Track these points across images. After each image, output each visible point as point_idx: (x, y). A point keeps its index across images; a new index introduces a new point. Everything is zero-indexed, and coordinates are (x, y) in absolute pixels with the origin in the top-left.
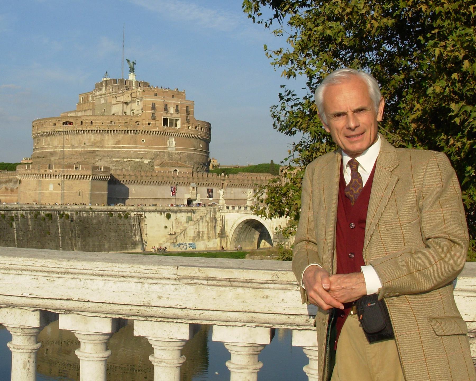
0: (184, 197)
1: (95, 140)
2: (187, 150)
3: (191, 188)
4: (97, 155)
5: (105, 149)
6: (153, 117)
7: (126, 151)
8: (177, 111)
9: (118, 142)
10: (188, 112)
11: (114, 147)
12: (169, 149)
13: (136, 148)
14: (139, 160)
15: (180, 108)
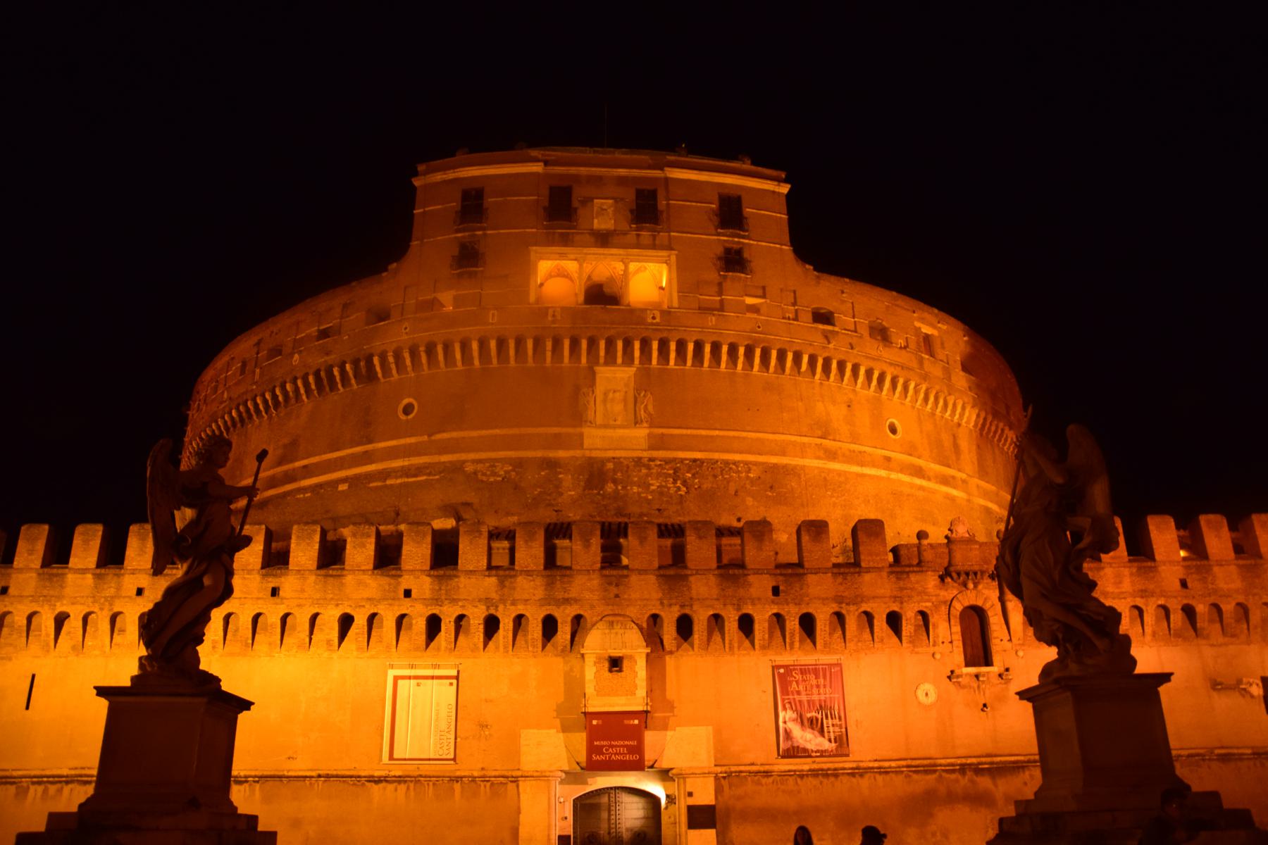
3: (591, 672)
12: (587, 443)
13: (367, 458)
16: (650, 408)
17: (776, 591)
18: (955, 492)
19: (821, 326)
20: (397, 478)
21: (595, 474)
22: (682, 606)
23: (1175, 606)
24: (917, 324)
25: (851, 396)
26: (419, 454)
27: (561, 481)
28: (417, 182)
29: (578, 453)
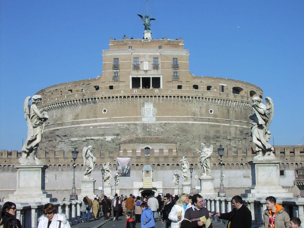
0: (132, 185)
1: (56, 116)
2: (178, 119)
3: (144, 173)
4: (58, 136)
5: (64, 127)
6: (116, 78)
7: (85, 127)
8: (156, 67)
9: (77, 116)
10: (176, 66)
11: (73, 123)
12: (143, 119)
13: (96, 121)
14: (98, 138)
15: (160, 61)
16: (156, 112)
17: (173, 160)
18: (226, 125)
19: (195, 90)
20: (103, 127)
21: (145, 127)
22: (158, 163)
23: (239, 164)
24: (220, 84)
25: (201, 105)
26: (108, 122)
27: (137, 128)
28: (103, 55)
29: (141, 122)
